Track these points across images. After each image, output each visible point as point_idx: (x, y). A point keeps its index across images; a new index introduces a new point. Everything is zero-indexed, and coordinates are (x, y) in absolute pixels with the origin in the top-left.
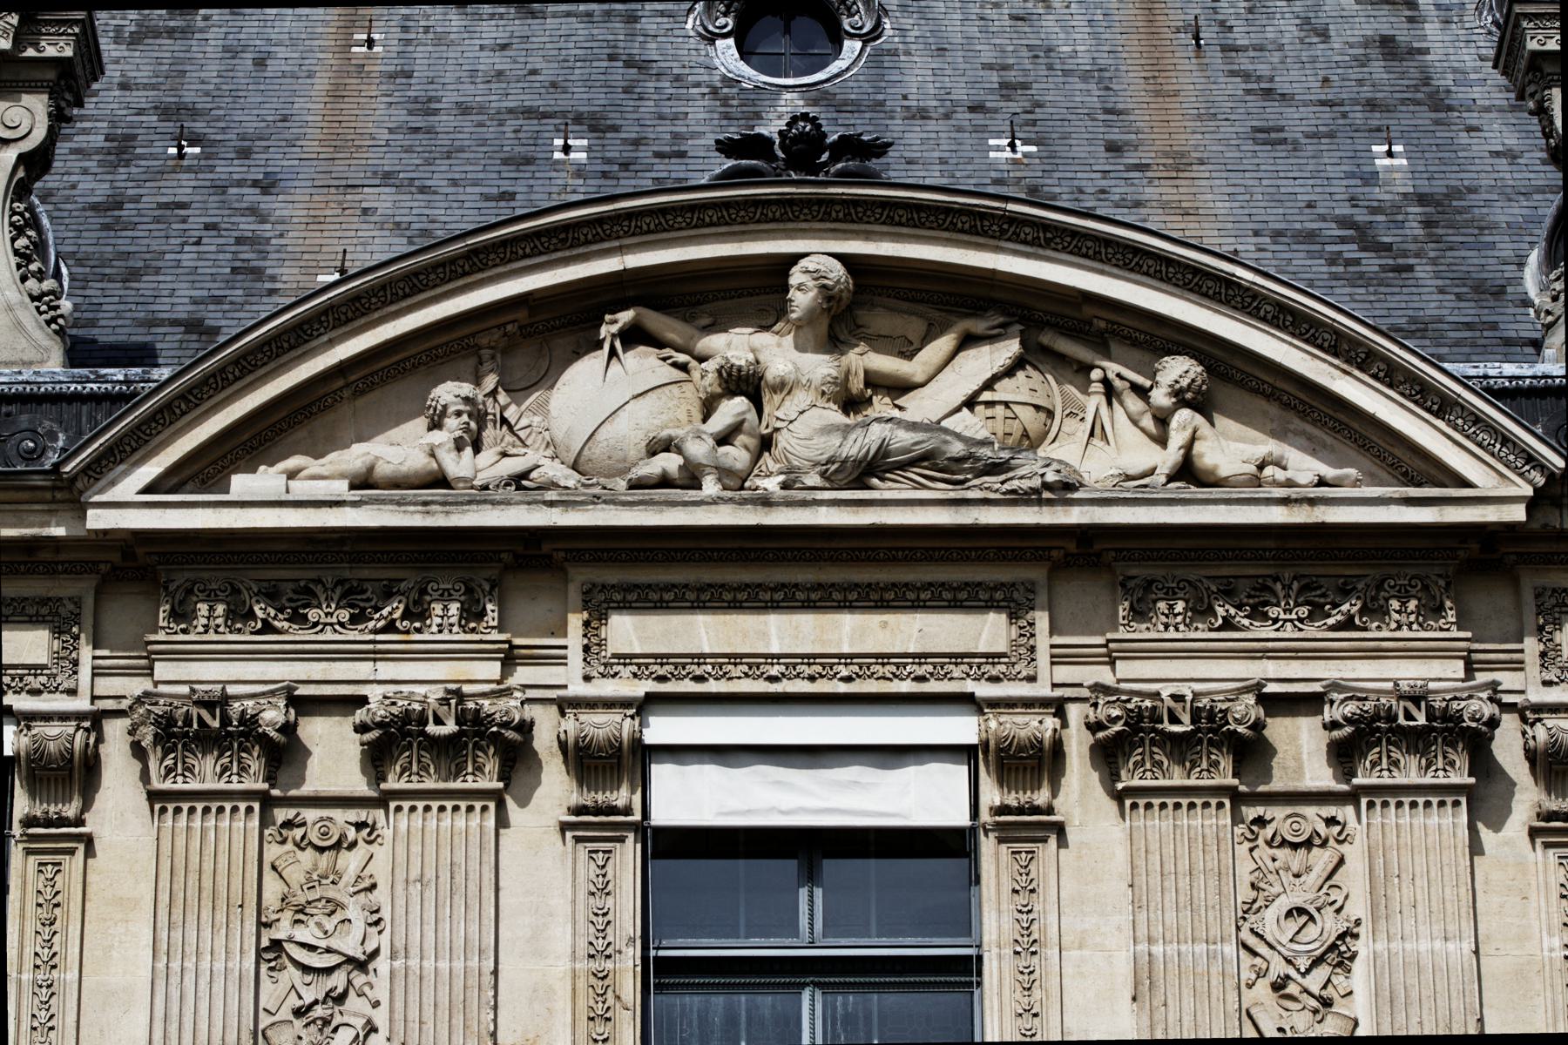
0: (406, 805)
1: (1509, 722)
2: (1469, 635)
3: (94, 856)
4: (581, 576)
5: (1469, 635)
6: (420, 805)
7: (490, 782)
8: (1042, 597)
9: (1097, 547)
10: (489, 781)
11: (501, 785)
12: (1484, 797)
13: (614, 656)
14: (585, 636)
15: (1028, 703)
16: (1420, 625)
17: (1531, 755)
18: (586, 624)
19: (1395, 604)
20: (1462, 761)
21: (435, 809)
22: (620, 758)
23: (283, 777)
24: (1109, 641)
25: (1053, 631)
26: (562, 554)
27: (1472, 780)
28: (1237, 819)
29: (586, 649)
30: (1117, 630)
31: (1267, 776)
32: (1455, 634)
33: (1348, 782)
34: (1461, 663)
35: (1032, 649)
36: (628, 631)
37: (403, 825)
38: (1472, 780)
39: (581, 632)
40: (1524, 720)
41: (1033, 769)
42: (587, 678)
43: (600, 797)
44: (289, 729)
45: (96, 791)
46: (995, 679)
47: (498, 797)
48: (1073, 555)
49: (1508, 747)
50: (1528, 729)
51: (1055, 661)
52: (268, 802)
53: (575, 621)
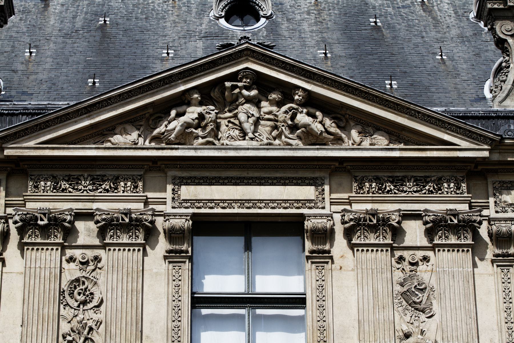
0: (112, 248)
1: (485, 224)
2: (470, 195)
3: (5, 266)
4: (171, 173)
5: (470, 195)
6: (117, 248)
7: (141, 241)
8: (327, 181)
9: (345, 165)
10: (141, 241)
11: (144, 242)
12: (477, 248)
13: (183, 200)
14: (173, 194)
15: (321, 216)
16: (455, 192)
17: (490, 235)
18: (173, 190)
19: (446, 185)
20: (470, 236)
21: (117, 250)
22: (184, 234)
23: (69, 239)
24: (349, 197)
25: (331, 192)
26: (163, 166)
27: (473, 243)
28: (393, 255)
29: (173, 198)
30: (352, 192)
31: (403, 241)
32: (466, 195)
33: (431, 243)
34: (468, 205)
35: (324, 199)
36: (188, 192)
37: (115, 257)
38: (473, 243)
39: (171, 193)
40: (489, 223)
41: (323, 238)
42: (173, 208)
43: (177, 247)
44: (71, 222)
45: (8, 244)
46: (310, 208)
47: (144, 246)
48: (338, 168)
49: (483, 231)
50: (490, 226)
51: (332, 203)
52: (64, 248)
53: (169, 187)
